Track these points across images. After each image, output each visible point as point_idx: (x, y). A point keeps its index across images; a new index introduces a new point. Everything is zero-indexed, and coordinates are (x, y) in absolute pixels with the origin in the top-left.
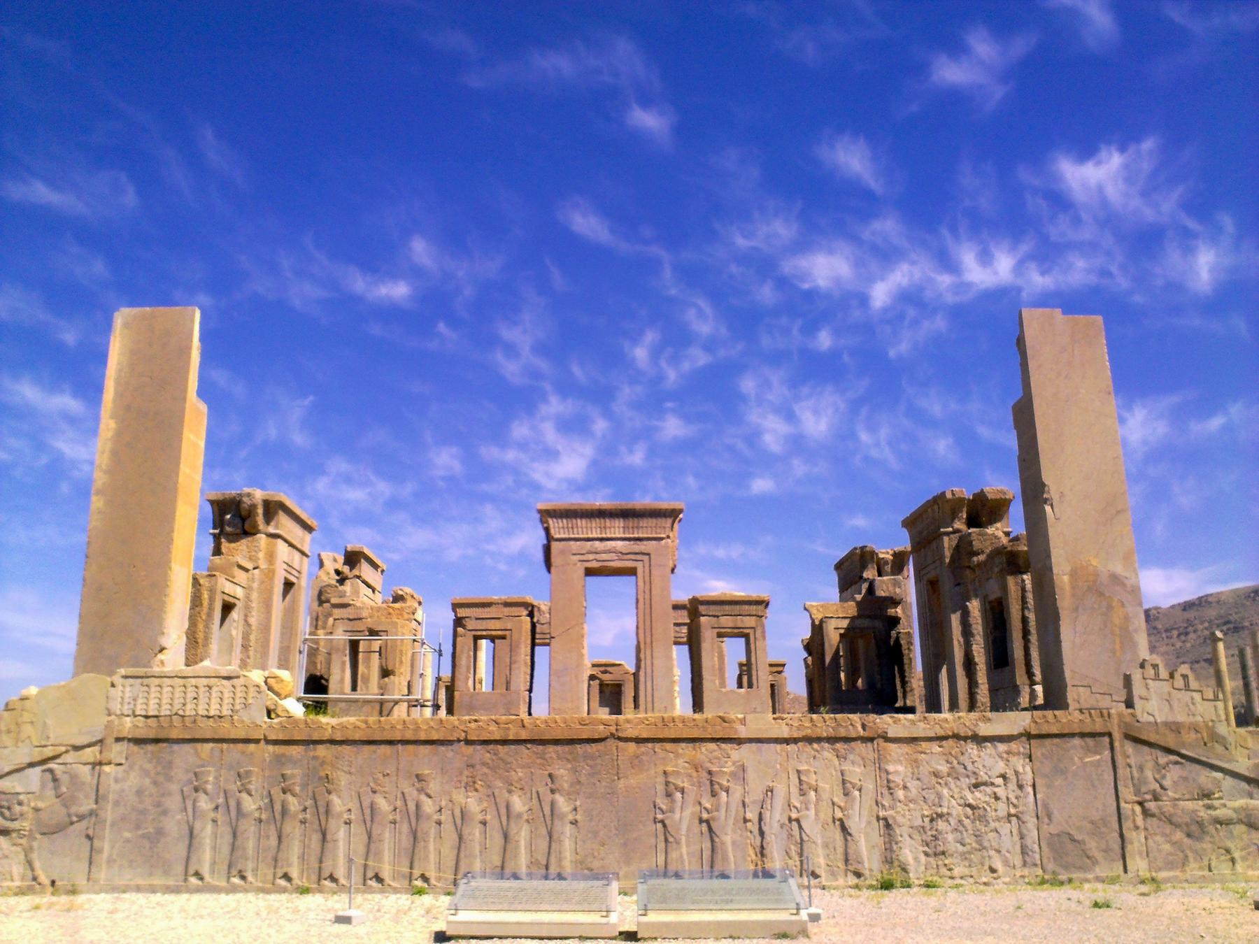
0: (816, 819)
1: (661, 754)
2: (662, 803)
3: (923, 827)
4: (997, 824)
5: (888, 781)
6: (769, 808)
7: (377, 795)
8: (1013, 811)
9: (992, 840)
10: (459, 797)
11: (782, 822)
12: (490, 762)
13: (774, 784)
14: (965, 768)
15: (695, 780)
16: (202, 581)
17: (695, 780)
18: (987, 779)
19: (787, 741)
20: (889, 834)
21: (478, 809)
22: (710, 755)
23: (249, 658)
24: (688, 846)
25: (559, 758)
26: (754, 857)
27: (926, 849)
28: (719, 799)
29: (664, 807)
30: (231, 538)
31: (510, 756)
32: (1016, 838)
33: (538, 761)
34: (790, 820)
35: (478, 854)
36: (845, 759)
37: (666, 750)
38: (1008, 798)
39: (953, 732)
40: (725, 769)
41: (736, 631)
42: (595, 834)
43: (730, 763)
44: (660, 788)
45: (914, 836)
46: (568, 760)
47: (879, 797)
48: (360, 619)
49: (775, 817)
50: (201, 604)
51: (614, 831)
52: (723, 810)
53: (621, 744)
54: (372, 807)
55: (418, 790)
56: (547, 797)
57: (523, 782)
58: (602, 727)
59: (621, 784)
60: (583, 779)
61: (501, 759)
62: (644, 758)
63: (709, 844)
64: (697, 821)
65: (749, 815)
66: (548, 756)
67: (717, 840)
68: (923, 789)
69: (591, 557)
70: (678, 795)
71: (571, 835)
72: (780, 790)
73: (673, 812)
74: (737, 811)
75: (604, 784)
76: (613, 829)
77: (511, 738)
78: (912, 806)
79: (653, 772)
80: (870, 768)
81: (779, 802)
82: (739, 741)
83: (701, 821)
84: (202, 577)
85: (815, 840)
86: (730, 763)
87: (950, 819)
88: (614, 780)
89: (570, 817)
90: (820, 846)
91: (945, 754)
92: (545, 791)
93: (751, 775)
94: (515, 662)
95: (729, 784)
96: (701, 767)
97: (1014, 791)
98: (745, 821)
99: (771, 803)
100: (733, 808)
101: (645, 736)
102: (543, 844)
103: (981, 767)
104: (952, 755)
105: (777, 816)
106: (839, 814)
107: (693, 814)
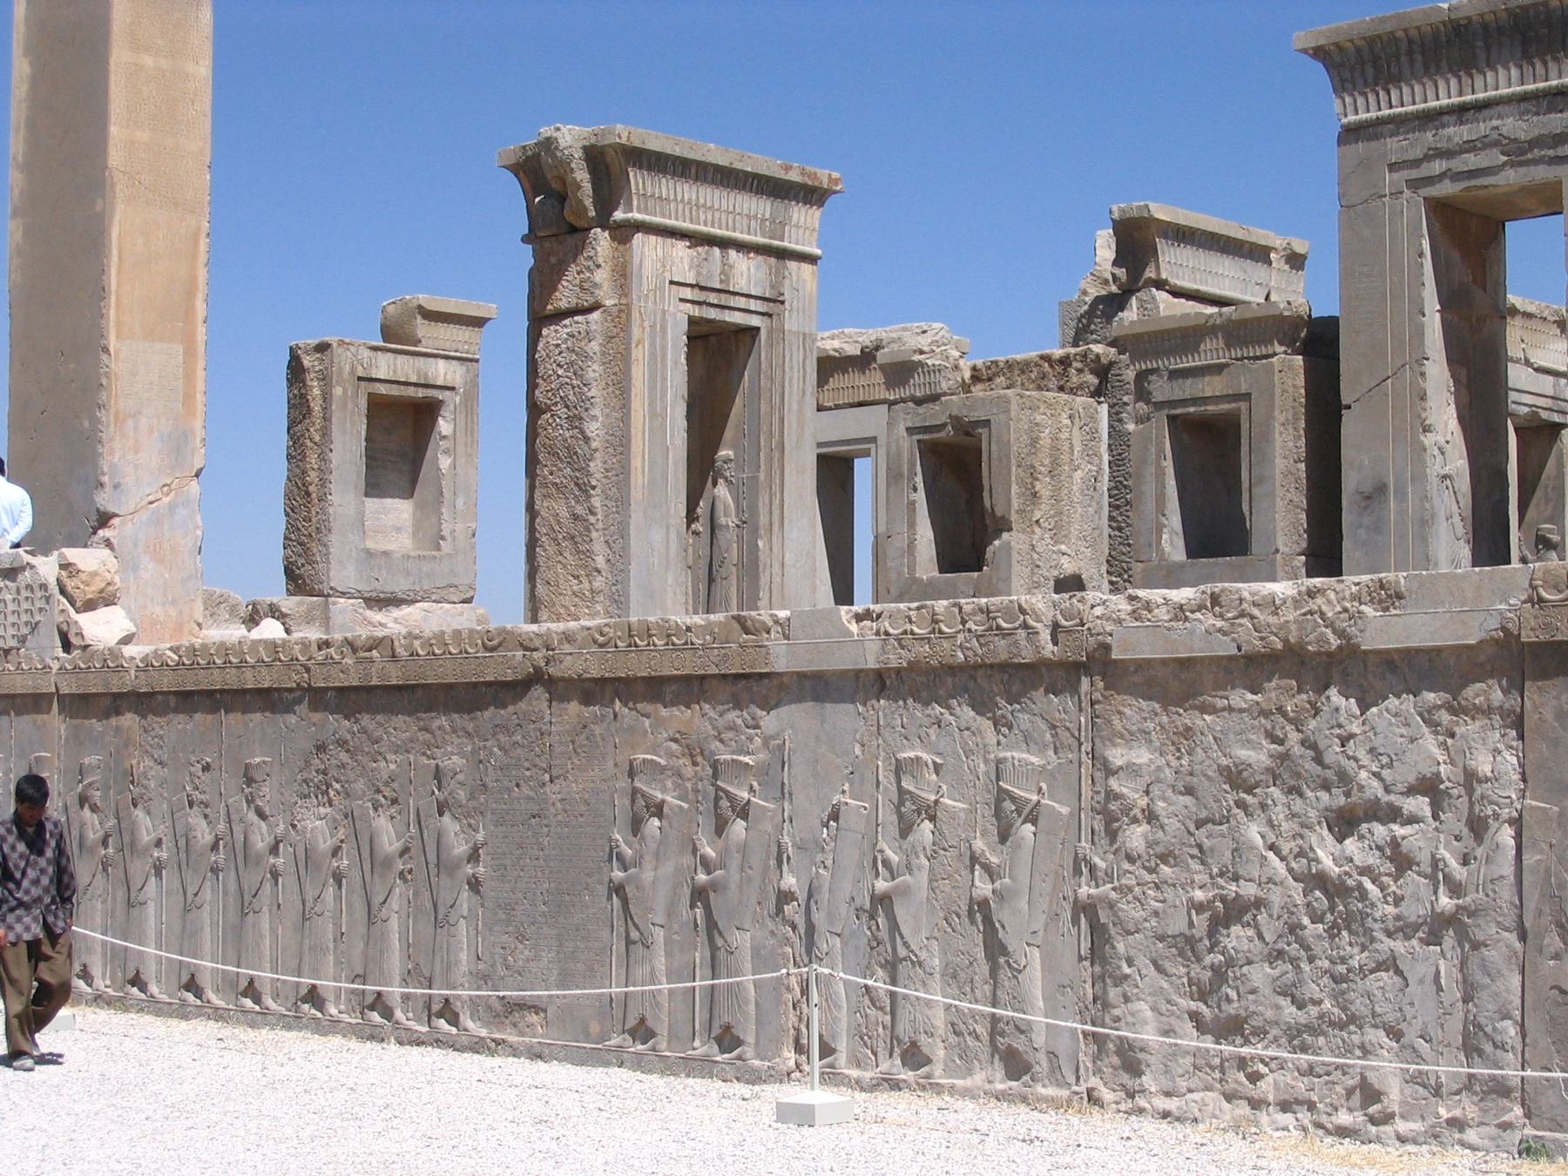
4: (1399, 946)
5: (1111, 796)
8: (1445, 902)
9: (1379, 994)
11: (858, 902)
14: (1318, 759)
16: (307, 361)
17: (689, 785)
18: (1380, 793)
23: (593, 513)
24: (668, 954)
25: (454, 731)
30: (547, 245)
32: (1453, 993)
35: (331, 946)
36: (1010, 728)
38: (1435, 862)
39: (1286, 641)
40: (746, 759)
44: (622, 802)
45: (1167, 965)
48: (934, 398)
50: (309, 411)
57: (395, 785)
67: (720, 942)
68: (1200, 824)
69: (1438, 166)
79: (611, 764)
84: (307, 352)
85: (923, 955)
86: (758, 741)
87: (1262, 918)
91: (1266, 714)
94: (1261, 480)
96: (702, 753)
97: (1458, 838)
103: (1362, 754)
104: (1284, 714)
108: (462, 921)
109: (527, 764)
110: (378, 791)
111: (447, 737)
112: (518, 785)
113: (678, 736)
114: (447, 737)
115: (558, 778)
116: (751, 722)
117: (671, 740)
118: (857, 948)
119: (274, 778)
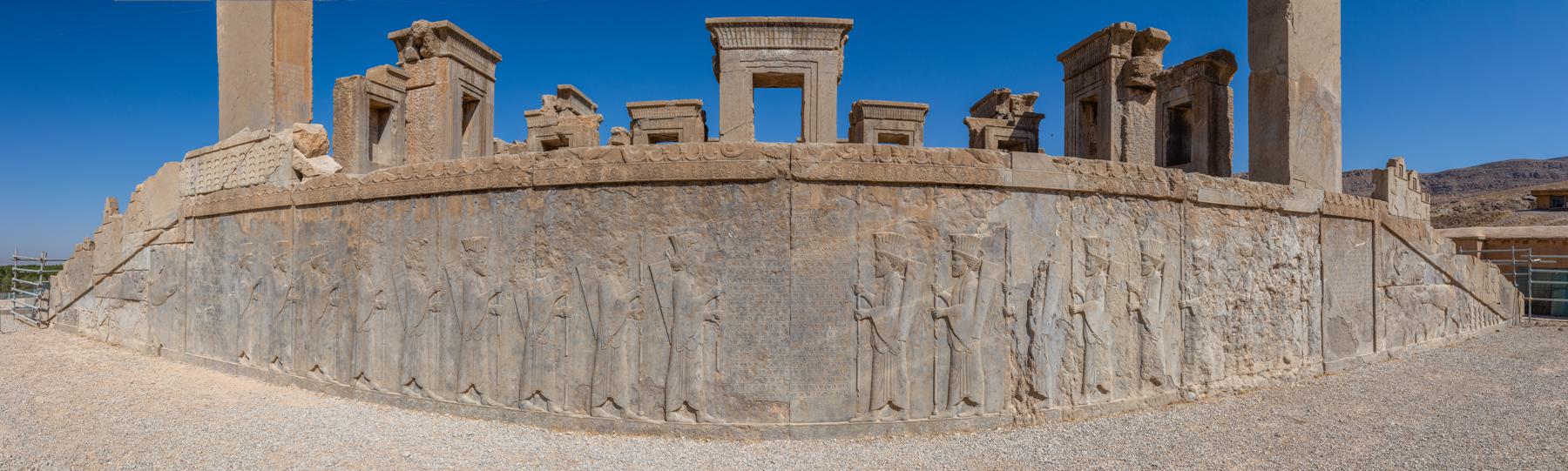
0: (1106, 311)
1: (869, 208)
2: (870, 288)
3: (1226, 318)
6: (1042, 295)
7: (412, 272)
10: (525, 275)
11: (1058, 316)
12: (571, 220)
13: (1051, 259)
15: (926, 251)
17: (926, 251)
19: (1071, 194)
20: (1191, 328)
21: (552, 295)
22: (952, 213)
25: (686, 213)
26: (1015, 371)
27: (1226, 343)
28: (964, 283)
29: (871, 296)
31: (603, 210)
33: (650, 217)
34: (1071, 312)
37: (878, 202)
40: (976, 235)
41: (896, 133)
42: (750, 340)
43: (984, 226)
44: (866, 263)
46: (702, 216)
47: (1183, 281)
49: (1051, 308)
51: (782, 335)
52: (971, 302)
53: (799, 189)
54: (410, 291)
55: (465, 265)
56: (667, 278)
57: (624, 252)
58: (763, 161)
59: (797, 257)
60: (728, 247)
61: (586, 214)
62: (838, 214)
63: (946, 354)
64: (928, 318)
65: (1011, 307)
66: (667, 208)
67: (959, 347)
70: (897, 275)
71: (706, 339)
72: (1059, 272)
73: (888, 305)
74: (993, 301)
75: (765, 256)
76: (780, 332)
77: (603, 179)
78: (1216, 290)
79: (853, 237)
80: (1175, 239)
81: (1056, 285)
82: (1002, 189)
83: (934, 317)
86: (984, 226)
88: (784, 251)
89: (706, 311)
90: (1109, 350)
92: (660, 266)
93: (1017, 244)
95: (982, 258)
98: (1005, 314)
99: (1045, 288)
100: (987, 296)
101: (841, 176)
102: (658, 353)
105: (1052, 308)
106: (1135, 304)
107: (920, 306)
108: (700, 348)
109: (767, 237)
110: (605, 256)
111: (679, 218)
112: (757, 251)
113: (915, 220)
114: (679, 218)
115: (799, 246)
116: (977, 213)
117: (910, 222)
118: (1058, 342)
119: (491, 250)
